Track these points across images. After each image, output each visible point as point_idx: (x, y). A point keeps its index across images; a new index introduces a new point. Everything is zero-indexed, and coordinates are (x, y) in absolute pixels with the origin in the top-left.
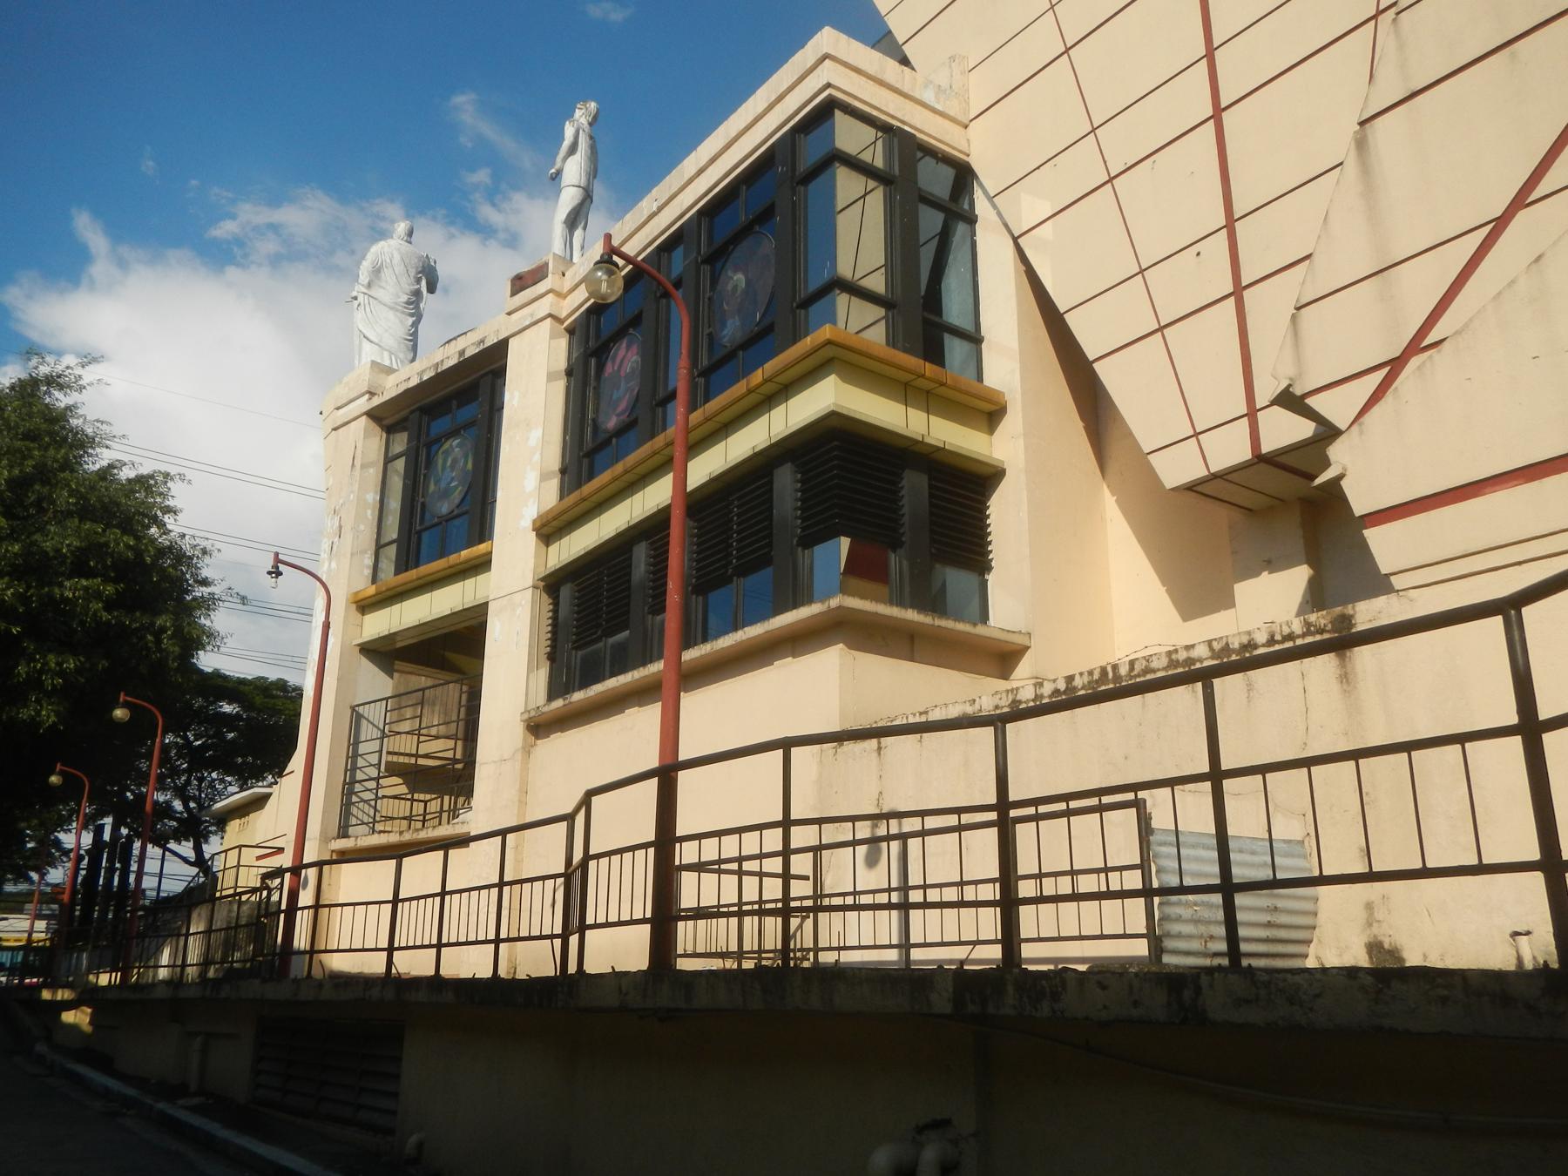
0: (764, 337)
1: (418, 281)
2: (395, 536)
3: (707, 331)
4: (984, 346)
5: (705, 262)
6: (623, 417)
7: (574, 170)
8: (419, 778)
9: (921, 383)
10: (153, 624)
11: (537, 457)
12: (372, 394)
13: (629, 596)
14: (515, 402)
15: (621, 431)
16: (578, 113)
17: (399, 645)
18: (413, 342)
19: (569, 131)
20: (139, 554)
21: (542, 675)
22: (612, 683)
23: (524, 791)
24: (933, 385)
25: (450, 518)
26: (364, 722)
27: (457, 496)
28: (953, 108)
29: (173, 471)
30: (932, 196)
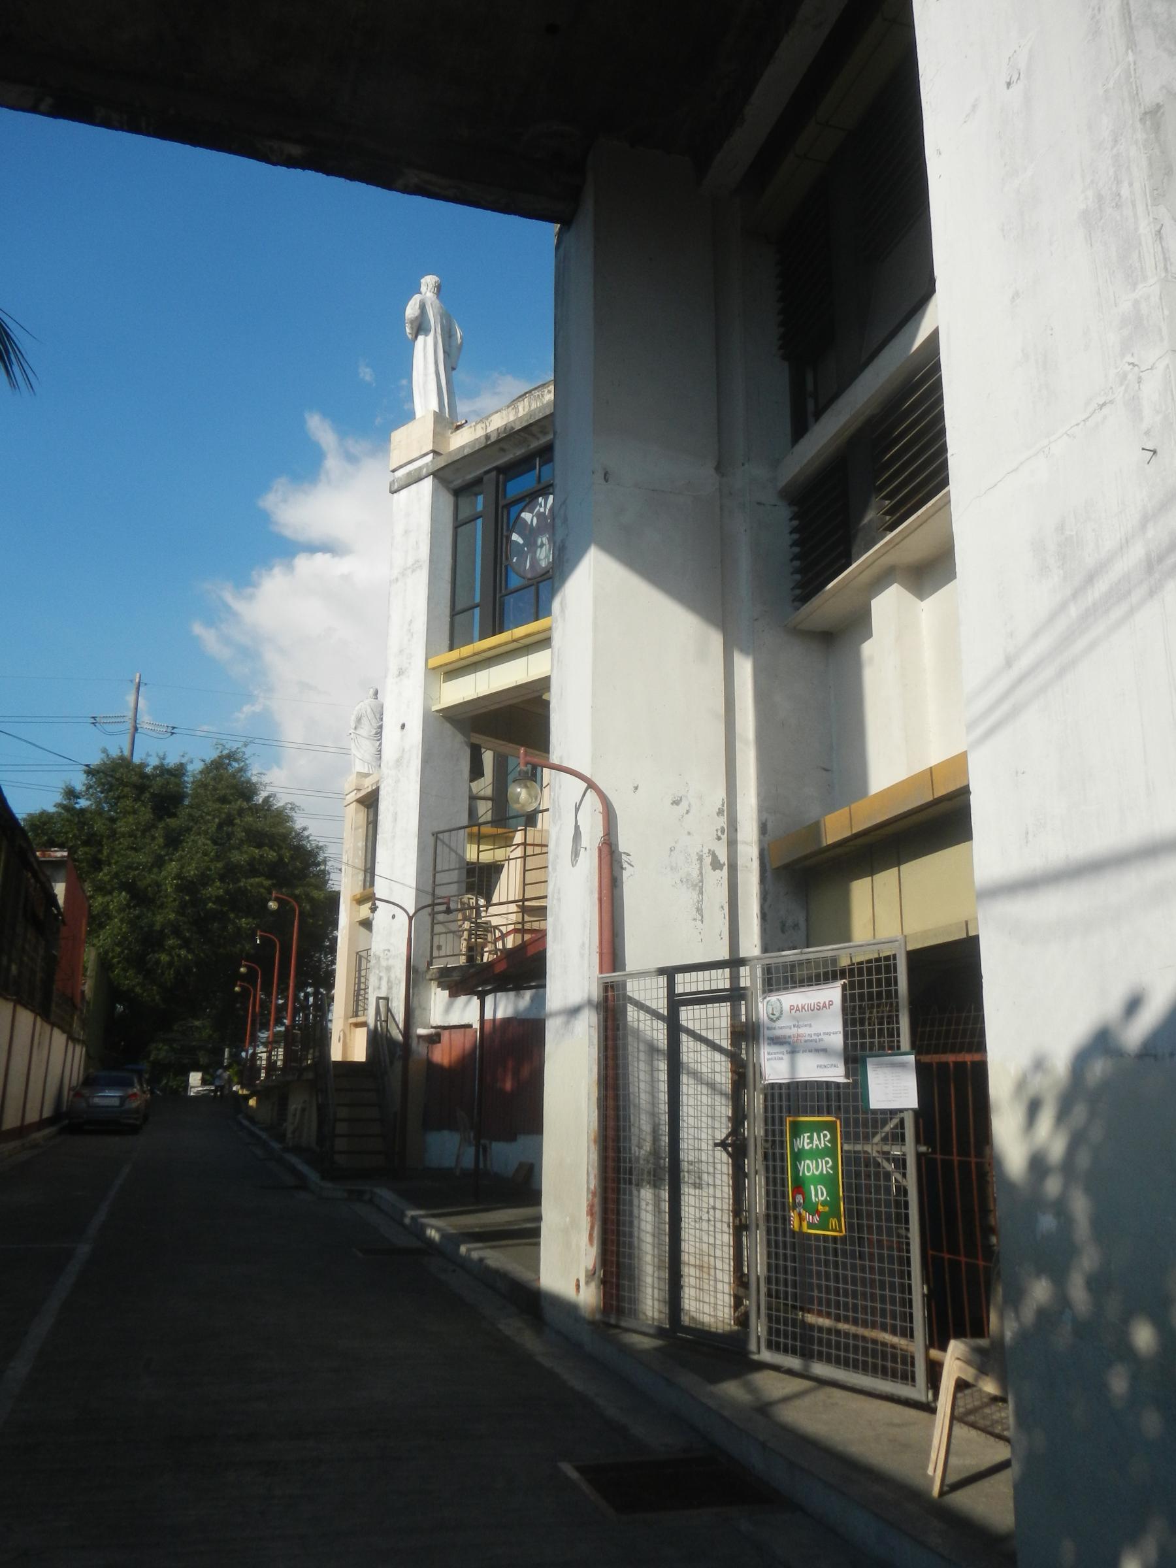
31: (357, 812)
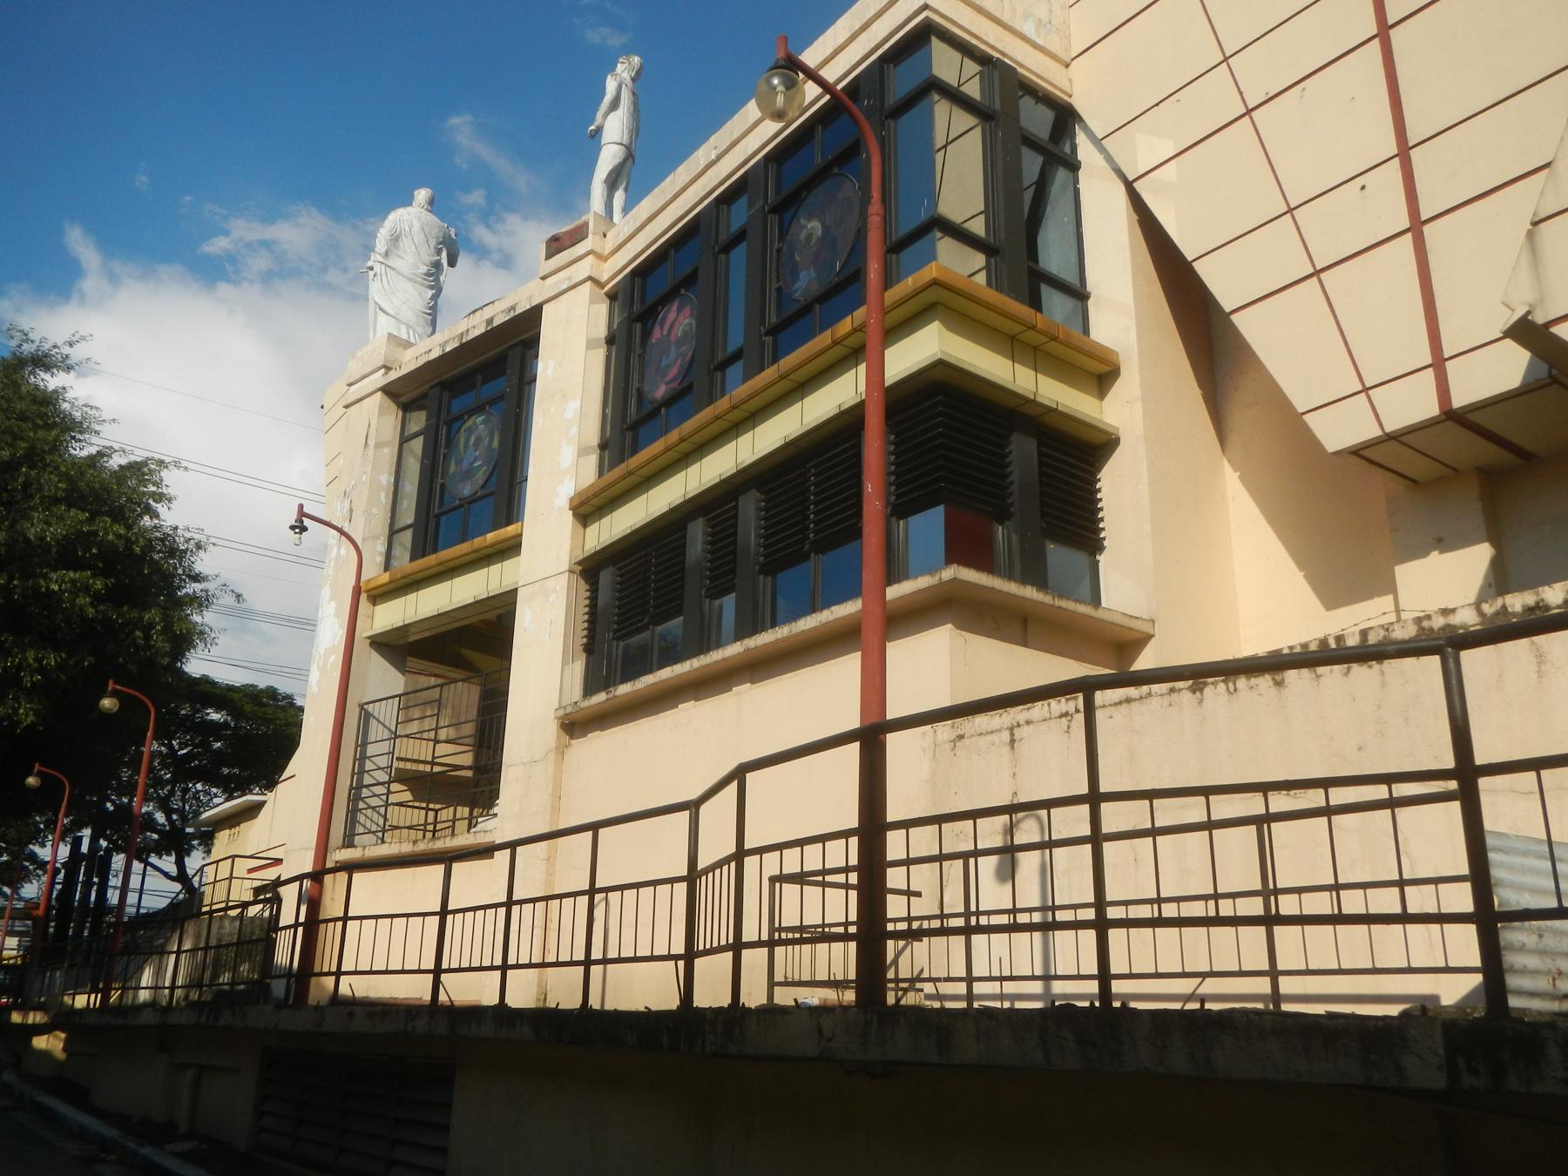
0: (844, 288)
1: (439, 252)
2: (410, 520)
3: (775, 286)
4: (1090, 303)
5: (773, 210)
6: (675, 385)
7: (615, 127)
8: (431, 787)
9: (1032, 337)
10: (141, 619)
11: (574, 430)
12: (388, 369)
13: (682, 579)
14: (550, 372)
15: (670, 401)
16: (620, 68)
17: (412, 639)
18: (432, 315)
19: (611, 85)
20: (129, 543)
21: (578, 668)
22: (666, 673)
23: (557, 797)
24: (1041, 339)
25: (473, 500)
26: (373, 723)
27: (480, 477)
28: (1054, 47)
29: (167, 460)
30: (1034, 137)
31: (382, 411)
